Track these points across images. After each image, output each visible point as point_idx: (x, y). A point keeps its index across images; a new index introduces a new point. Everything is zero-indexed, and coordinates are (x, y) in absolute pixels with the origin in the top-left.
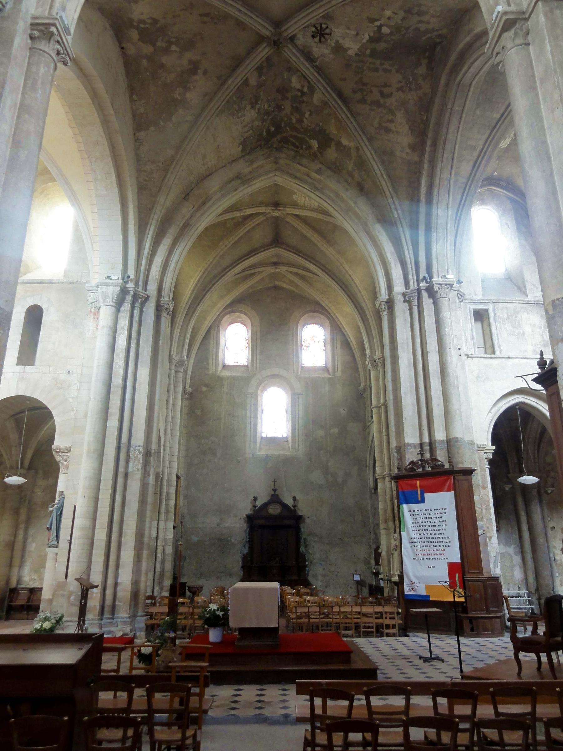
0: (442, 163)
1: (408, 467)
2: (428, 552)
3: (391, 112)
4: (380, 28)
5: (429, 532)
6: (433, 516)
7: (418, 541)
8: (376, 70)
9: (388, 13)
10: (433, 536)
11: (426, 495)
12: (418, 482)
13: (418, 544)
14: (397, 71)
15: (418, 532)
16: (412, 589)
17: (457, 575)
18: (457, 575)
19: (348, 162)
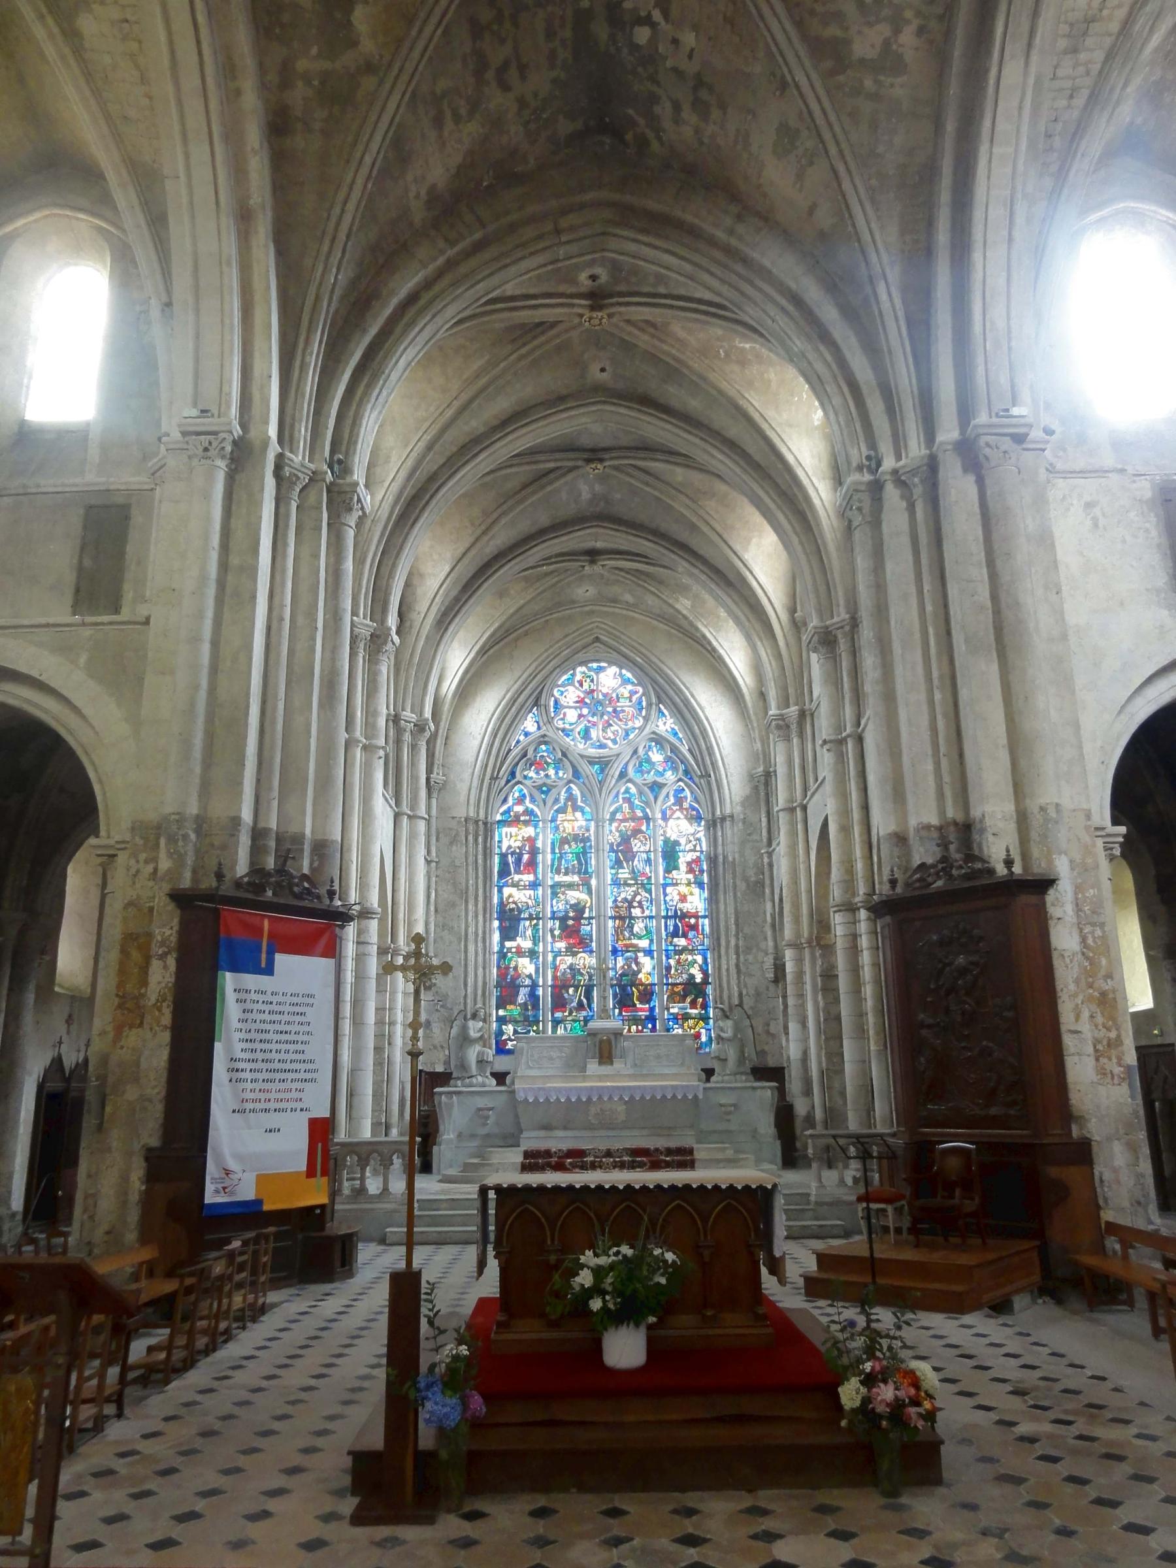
0: (467, 290)
1: (246, 879)
2: (268, 1096)
3: (474, 107)
4: (648, 21)
5: (274, 1047)
6: (287, 1008)
7: (248, 1066)
8: (550, 34)
9: (689, 39)
10: (282, 1056)
11: (279, 958)
12: (266, 923)
13: (247, 1075)
14: (554, 81)
15: (249, 1045)
16: (224, 1188)
17: (320, 1145)
18: (320, 1145)
19: (314, 51)
